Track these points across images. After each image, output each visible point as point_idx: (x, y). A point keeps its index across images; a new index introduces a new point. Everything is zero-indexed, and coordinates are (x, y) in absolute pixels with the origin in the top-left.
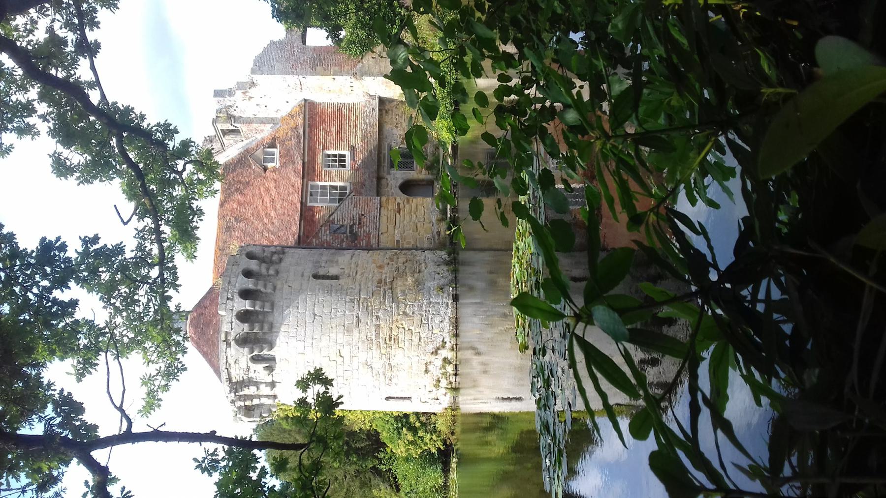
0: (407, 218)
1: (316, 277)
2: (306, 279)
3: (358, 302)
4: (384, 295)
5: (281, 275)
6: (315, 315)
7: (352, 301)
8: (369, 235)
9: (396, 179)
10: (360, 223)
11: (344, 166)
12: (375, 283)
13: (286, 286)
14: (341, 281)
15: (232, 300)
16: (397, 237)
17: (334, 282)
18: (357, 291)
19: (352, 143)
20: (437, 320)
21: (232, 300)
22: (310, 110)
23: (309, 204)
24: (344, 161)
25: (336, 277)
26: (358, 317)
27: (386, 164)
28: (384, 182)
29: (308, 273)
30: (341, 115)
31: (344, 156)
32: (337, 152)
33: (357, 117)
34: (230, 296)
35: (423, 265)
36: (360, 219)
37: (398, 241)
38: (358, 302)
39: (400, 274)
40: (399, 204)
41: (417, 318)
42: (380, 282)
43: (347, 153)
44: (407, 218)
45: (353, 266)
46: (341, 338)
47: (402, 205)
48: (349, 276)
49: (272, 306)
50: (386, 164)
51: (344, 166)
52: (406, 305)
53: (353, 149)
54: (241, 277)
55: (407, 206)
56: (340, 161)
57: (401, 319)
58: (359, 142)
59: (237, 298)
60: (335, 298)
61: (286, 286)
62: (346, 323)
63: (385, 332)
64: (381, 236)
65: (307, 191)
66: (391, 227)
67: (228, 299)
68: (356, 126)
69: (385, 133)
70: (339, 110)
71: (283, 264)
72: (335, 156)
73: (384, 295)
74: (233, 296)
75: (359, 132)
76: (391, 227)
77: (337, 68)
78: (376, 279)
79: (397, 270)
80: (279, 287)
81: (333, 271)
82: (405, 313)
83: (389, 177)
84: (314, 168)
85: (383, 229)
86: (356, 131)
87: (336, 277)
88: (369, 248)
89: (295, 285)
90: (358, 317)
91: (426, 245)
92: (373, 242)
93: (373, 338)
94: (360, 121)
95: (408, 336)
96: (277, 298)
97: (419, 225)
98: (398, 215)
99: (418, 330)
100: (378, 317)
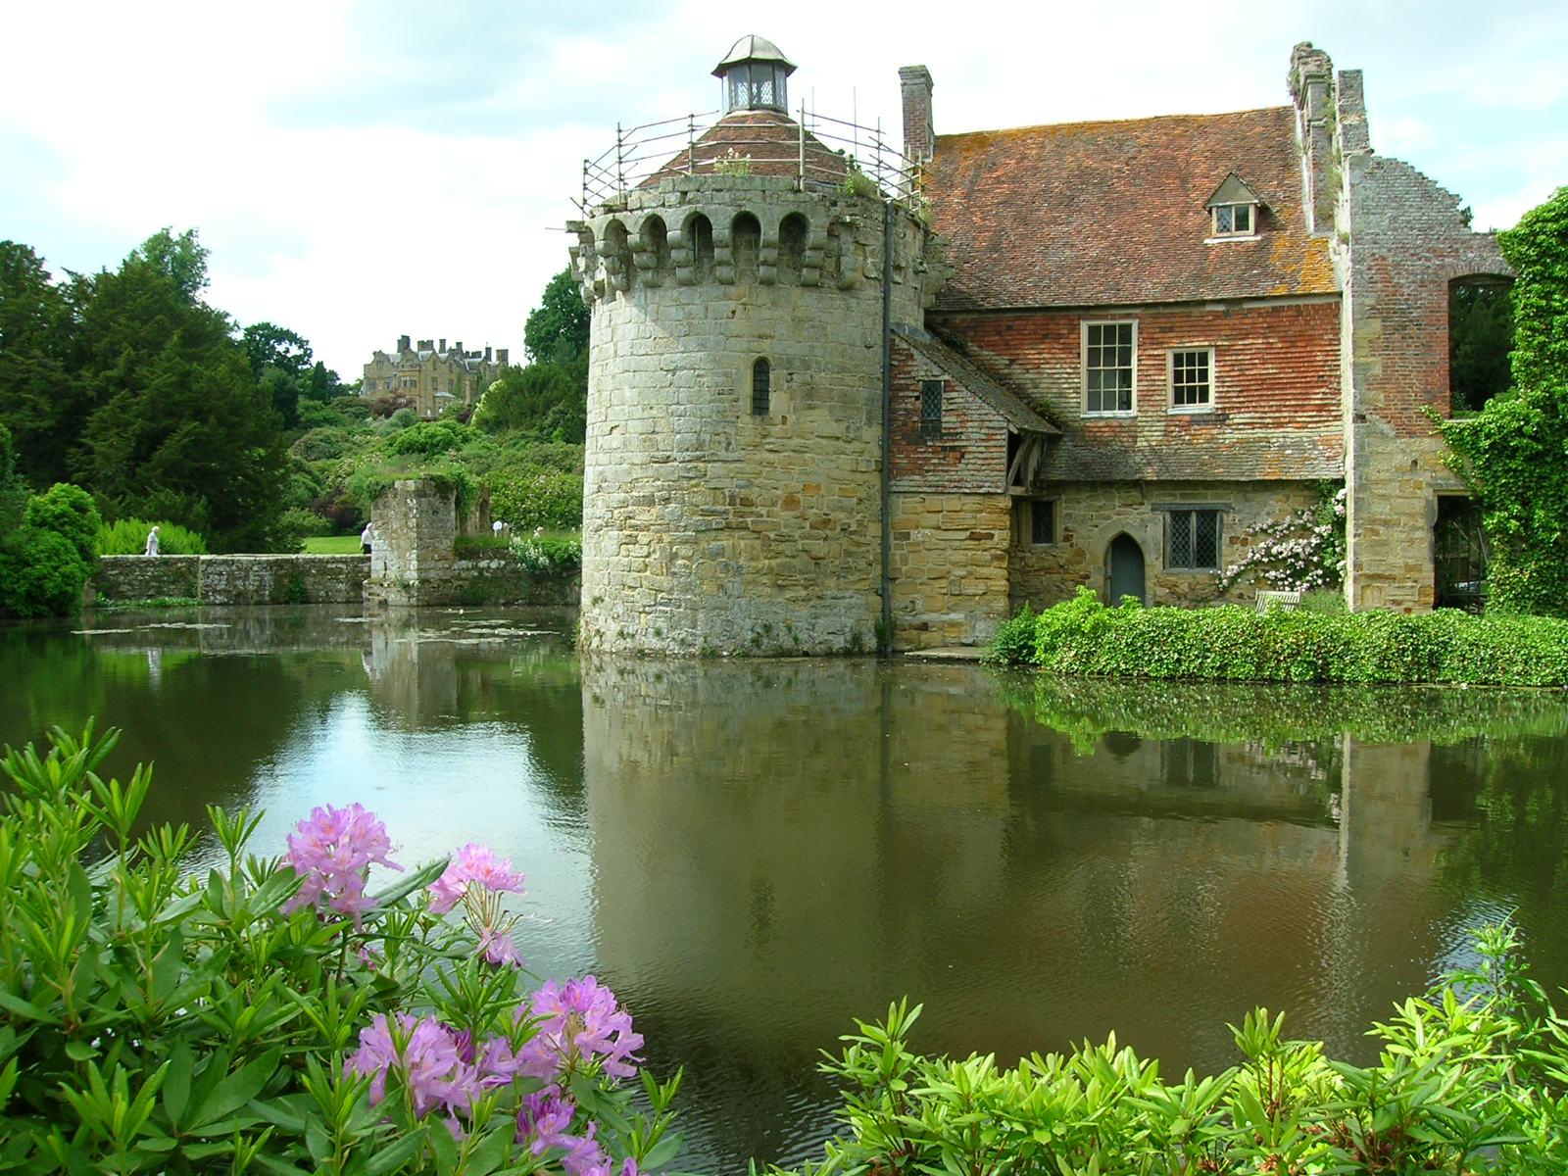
0: (959, 557)
1: (761, 368)
2: (755, 345)
3: (698, 459)
4: (713, 513)
5: (764, 291)
6: (674, 371)
7: (700, 446)
8: (919, 470)
9: (1144, 525)
10: (944, 448)
11: (1178, 400)
12: (743, 493)
13: (733, 305)
14: (747, 421)
15: (682, 202)
16: (916, 535)
17: (746, 404)
18: (723, 454)
19: (1237, 418)
20: (662, 624)
21: (682, 202)
22: (1317, 309)
23: (1084, 326)
24: (1191, 400)
25: (760, 405)
26: (667, 460)
27: (1179, 501)
28: (1135, 494)
29: (766, 348)
30: (1308, 387)
31: (1204, 398)
32: (1212, 381)
33: (1304, 426)
34: (690, 196)
35: (803, 593)
36: (953, 449)
37: (907, 536)
38: (698, 459)
39: (771, 542)
40: (991, 536)
41: (665, 582)
42: (746, 502)
43: (1211, 404)
44: (959, 557)
45: (796, 441)
46: (636, 427)
47: (988, 544)
48: (764, 437)
49: (687, 283)
50: (1179, 501)
51: (1178, 400)
52: (689, 558)
53: (1220, 418)
54: (732, 212)
55: (987, 555)
56: (1192, 390)
57: (663, 550)
58: (1237, 435)
59: (687, 209)
60: (706, 409)
61: (733, 305)
62: (659, 437)
63: (644, 516)
64: (917, 499)
65: (1114, 317)
66: (934, 519)
67: (685, 193)
68: (1280, 425)
69: (1260, 497)
70: (1322, 382)
71: (798, 291)
72: (1204, 375)
73: (713, 513)
74: (689, 202)
75: (1260, 433)
76: (934, 519)
77: (1378, 370)
78: (754, 494)
79: (781, 539)
80: (732, 290)
81: (777, 401)
82: (674, 557)
83: (1146, 508)
84: (1171, 329)
85: (934, 502)
86: (1265, 426)
87: (760, 405)
88: (887, 470)
89: (738, 325)
90: (667, 460)
91: (899, 600)
92: (904, 483)
93: (634, 494)
94: (1292, 433)
95: (638, 563)
96: (708, 290)
97: (943, 583)
98: (968, 533)
99: (645, 583)
100: (667, 500)
